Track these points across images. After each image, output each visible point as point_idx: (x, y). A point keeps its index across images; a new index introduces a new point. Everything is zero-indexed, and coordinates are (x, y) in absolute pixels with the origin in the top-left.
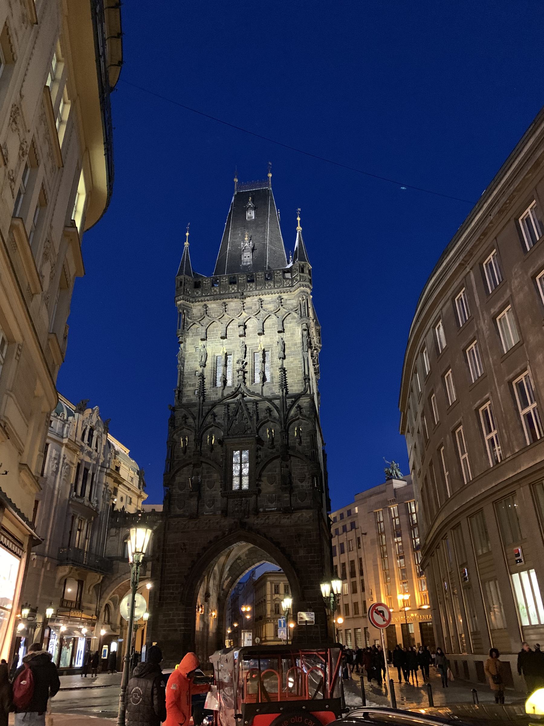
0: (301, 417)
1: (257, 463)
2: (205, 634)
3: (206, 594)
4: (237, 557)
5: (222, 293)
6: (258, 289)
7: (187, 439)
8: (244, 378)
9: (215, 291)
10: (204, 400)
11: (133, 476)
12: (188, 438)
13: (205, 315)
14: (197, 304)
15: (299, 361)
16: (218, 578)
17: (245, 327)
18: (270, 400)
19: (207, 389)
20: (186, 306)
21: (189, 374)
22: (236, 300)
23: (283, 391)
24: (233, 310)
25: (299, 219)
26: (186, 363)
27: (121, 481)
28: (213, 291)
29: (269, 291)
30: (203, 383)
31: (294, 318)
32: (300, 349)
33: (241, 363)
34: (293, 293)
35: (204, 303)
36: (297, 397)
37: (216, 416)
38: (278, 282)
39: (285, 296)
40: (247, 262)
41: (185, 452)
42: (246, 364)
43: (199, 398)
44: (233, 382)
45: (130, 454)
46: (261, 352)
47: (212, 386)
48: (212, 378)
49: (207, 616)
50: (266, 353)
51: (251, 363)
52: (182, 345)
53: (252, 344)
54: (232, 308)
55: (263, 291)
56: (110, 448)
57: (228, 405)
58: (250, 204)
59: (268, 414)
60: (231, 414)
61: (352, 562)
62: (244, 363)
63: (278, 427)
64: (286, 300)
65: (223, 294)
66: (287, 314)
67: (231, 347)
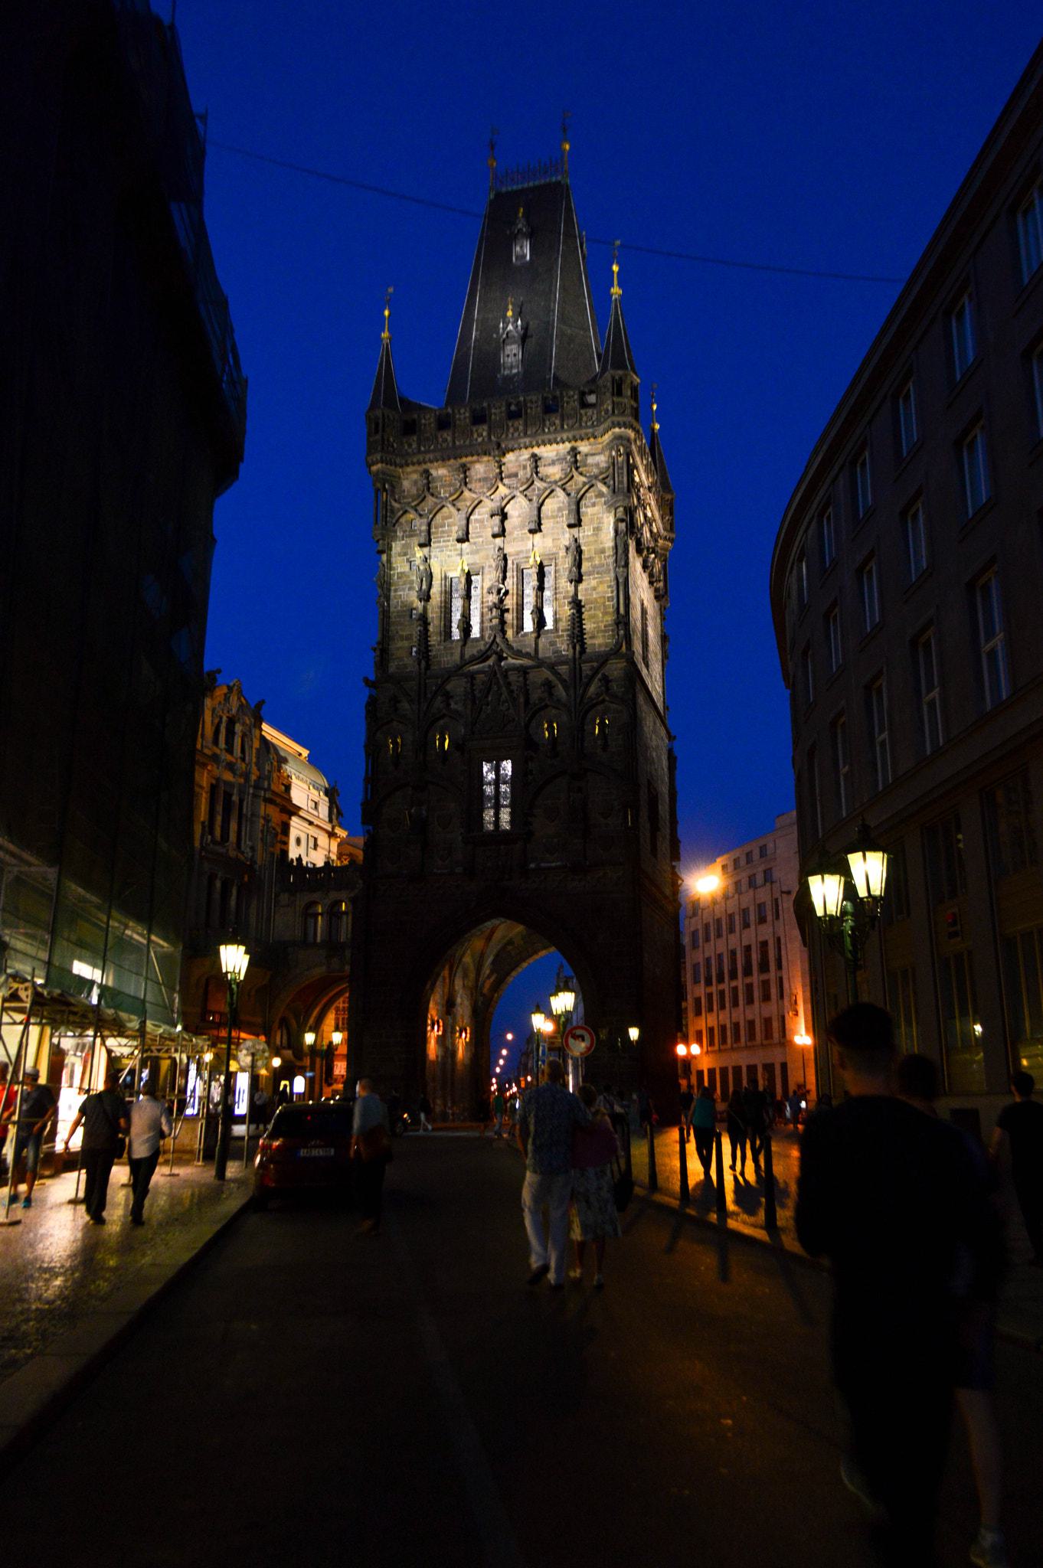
0: (607, 698)
3: (447, 1002)
4: (505, 941)
5: (457, 443)
6: (529, 433)
7: (399, 740)
8: (503, 622)
9: (445, 440)
10: (428, 667)
11: (316, 799)
12: (402, 739)
13: (426, 493)
14: (410, 469)
15: (609, 587)
16: (472, 976)
17: (504, 516)
18: (552, 667)
19: (434, 645)
20: (388, 475)
21: (399, 616)
22: (485, 459)
23: (574, 648)
24: (480, 480)
25: (615, 268)
26: (392, 594)
27: (295, 811)
28: (440, 440)
29: (551, 437)
30: (425, 634)
31: (600, 495)
32: (611, 560)
33: (495, 591)
34: (600, 440)
35: (424, 466)
36: (604, 658)
37: (452, 697)
38: (569, 417)
39: (584, 447)
40: (512, 367)
42: (507, 593)
43: (419, 664)
44: (482, 630)
45: (312, 760)
46: (535, 570)
47: (443, 638)
48: (443, 623)
49: (452, 1037)
50: (546, 569)
51: (515, 592)
53: (518, 553)
54: (478, 476)
55: (540, 439)
56: (268, 752)
57: (472, 676)
58: (520, 226)
59: (546, 695)
61: (764, 944)
62: (503, 591)
63: (565, 718)
64: (586, 455)
65: (460, 447)
66: (587, 487)
67: (477, 559)
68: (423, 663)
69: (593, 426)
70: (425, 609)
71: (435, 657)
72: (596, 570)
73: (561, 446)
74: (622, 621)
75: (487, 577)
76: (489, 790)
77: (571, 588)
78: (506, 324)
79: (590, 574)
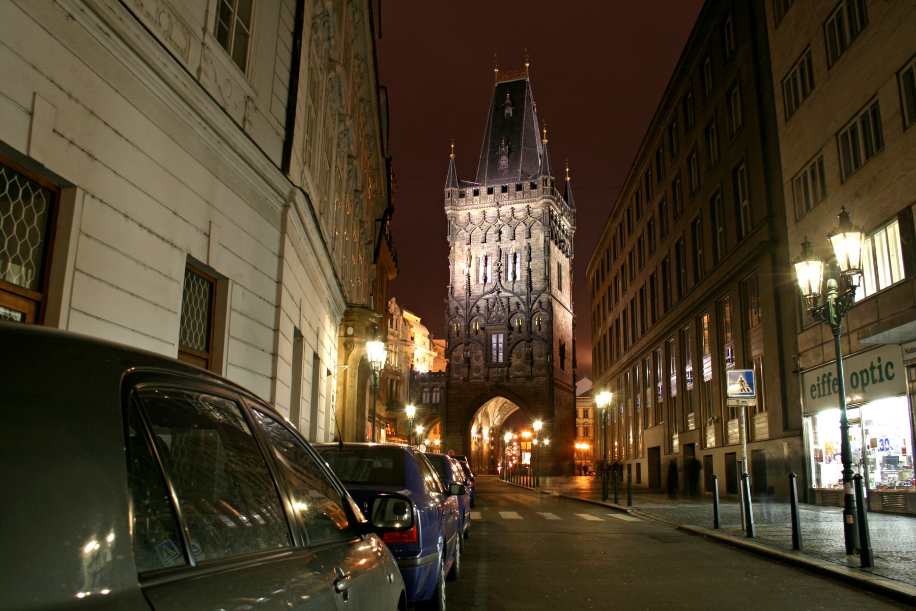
1: (509, 344)
2: (480, 453)
8: (500, 277)
9: (476, 201)
10: (470, 295)
17: (500, 233)
32: (543, 253)
33: (496, 264)
39: (532, 205)
40: (504, 166)
41: (458, 335)
42: (501, 265)
52: (452, 248)
60: (490, 307)
63: (524, 317)
67: (490, 250)
68: (468, 294)
69: (535, 197)
70: (469, 271)
71: (473, 290)
72: (537, 257)
73: (523, 204)
74: (547, 279)
75: (494, 258)
76: (494, 346)
77: (527, 263)
78: (502, 147)
79: (534, 258)
